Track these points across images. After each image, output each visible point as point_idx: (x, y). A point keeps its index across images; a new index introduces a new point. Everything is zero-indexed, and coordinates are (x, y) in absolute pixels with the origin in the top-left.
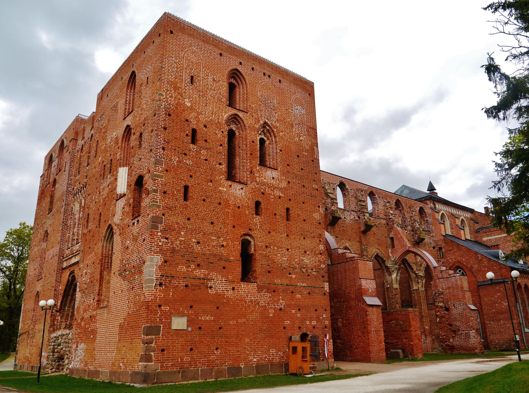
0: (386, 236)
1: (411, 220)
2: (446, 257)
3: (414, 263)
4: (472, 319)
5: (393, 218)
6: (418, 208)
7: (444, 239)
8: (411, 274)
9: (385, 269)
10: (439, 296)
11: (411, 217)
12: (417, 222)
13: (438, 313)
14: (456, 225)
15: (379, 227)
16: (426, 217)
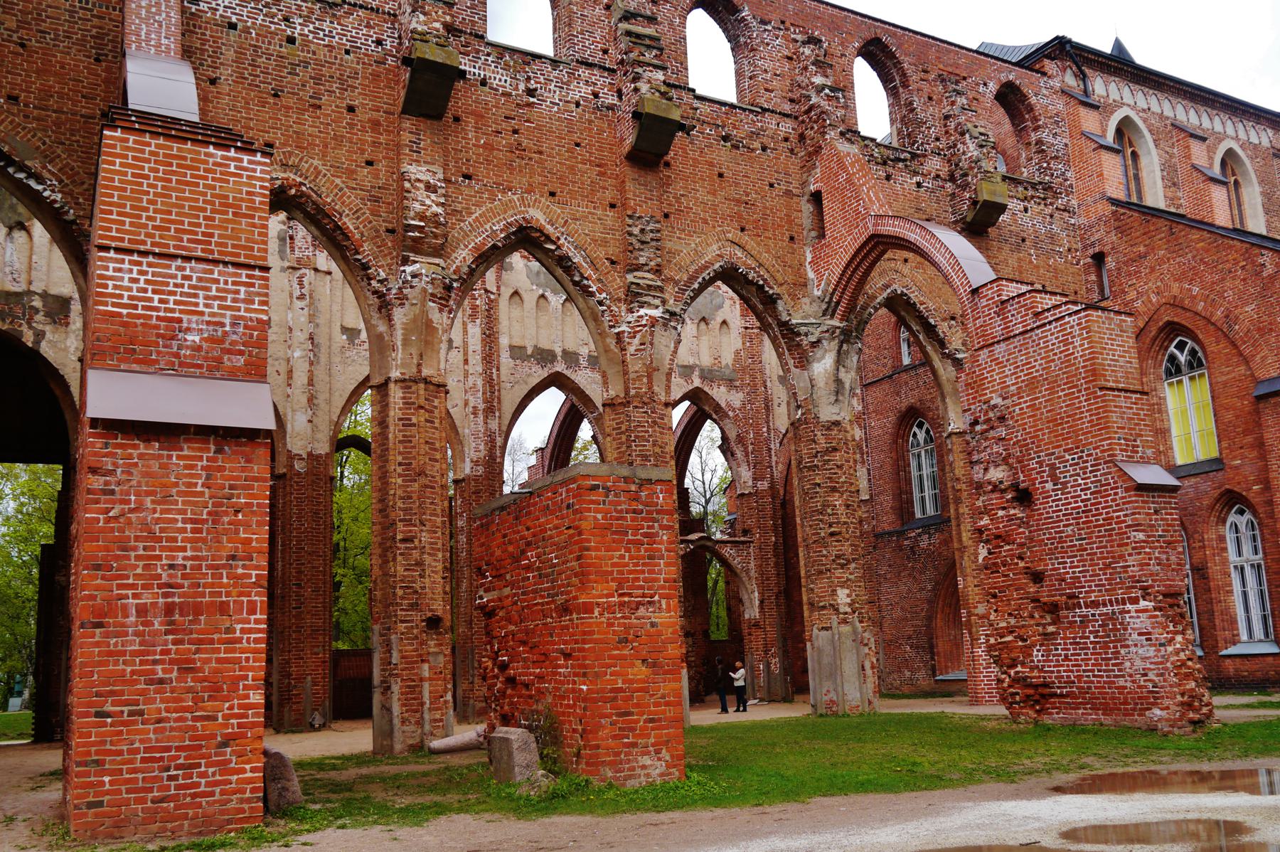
0: (788, 193)
1: (947, 132)
2: (1124, 292)
3: (953, 318)
4: (1141, 536)
5: (824, 104)
6: (991, 85)
7: (1114, 213)
8: (937, 363)
9: (784, 336)
10: (992, 434)
11: (947, 117)
12: (971, 137)
13: (985, 521)
14: (1194, 167)
15: (753, 150)
16: (1036, 129)
